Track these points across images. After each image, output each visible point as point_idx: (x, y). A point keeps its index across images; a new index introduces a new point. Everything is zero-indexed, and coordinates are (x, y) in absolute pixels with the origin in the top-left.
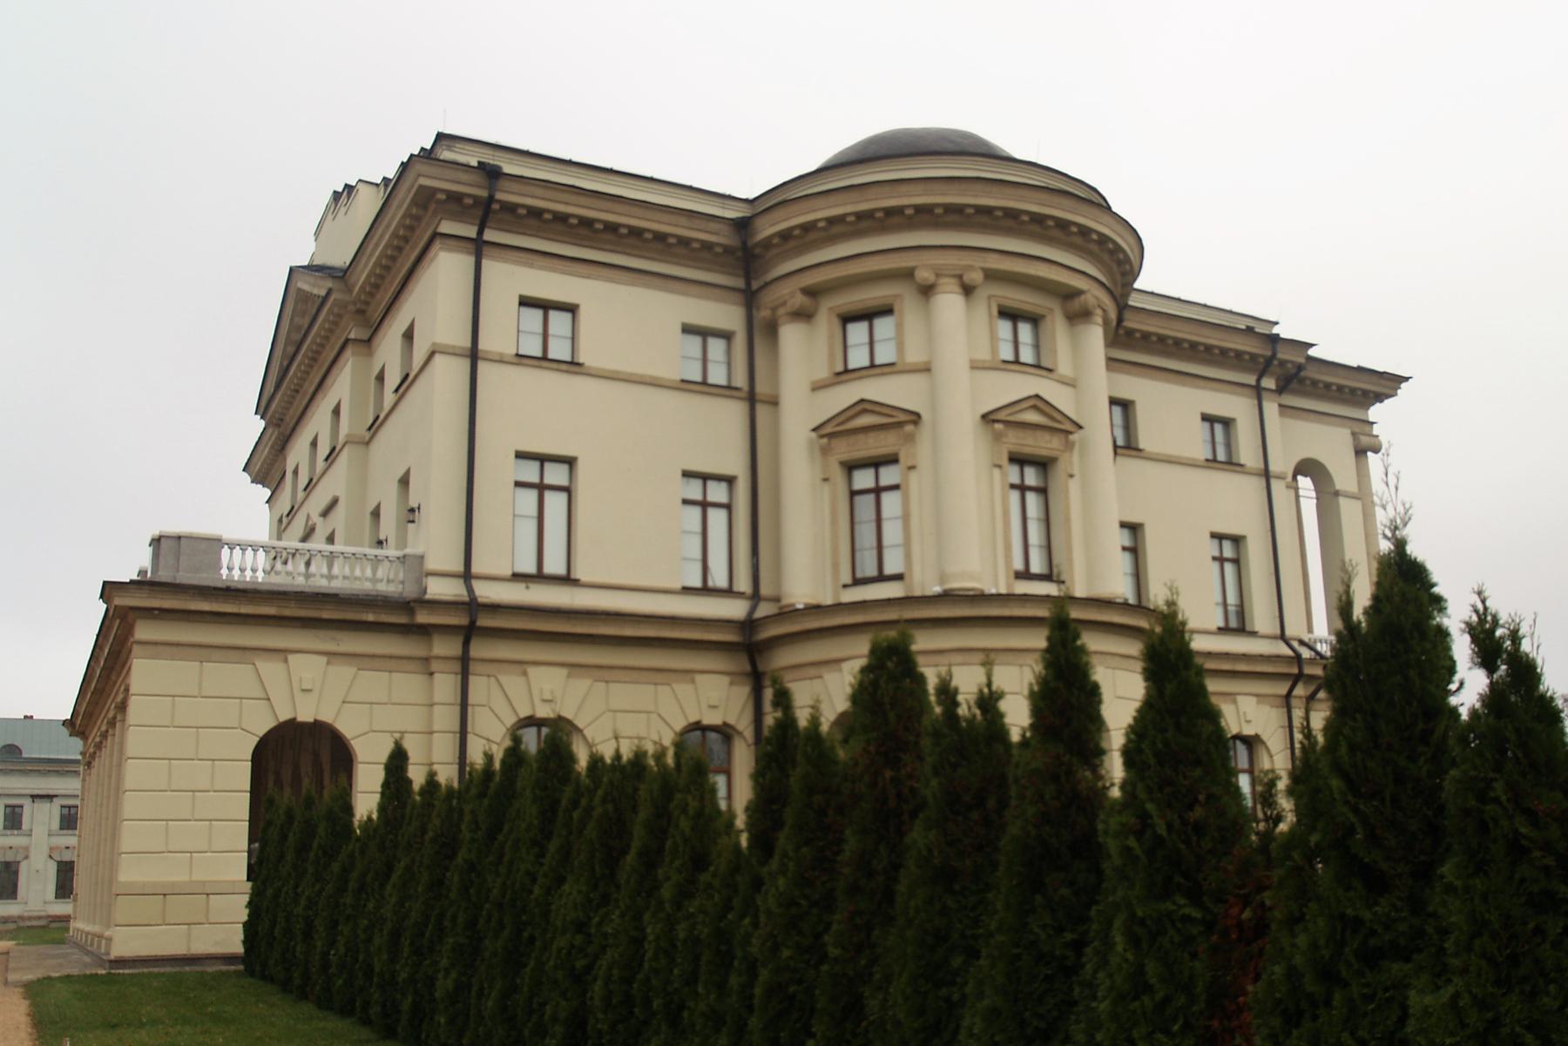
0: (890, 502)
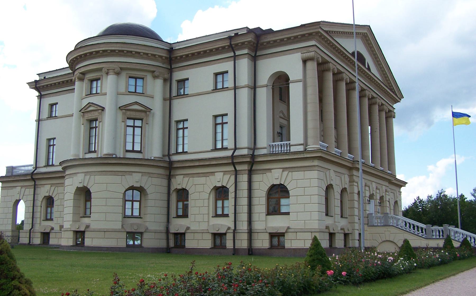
0: (138, 131)
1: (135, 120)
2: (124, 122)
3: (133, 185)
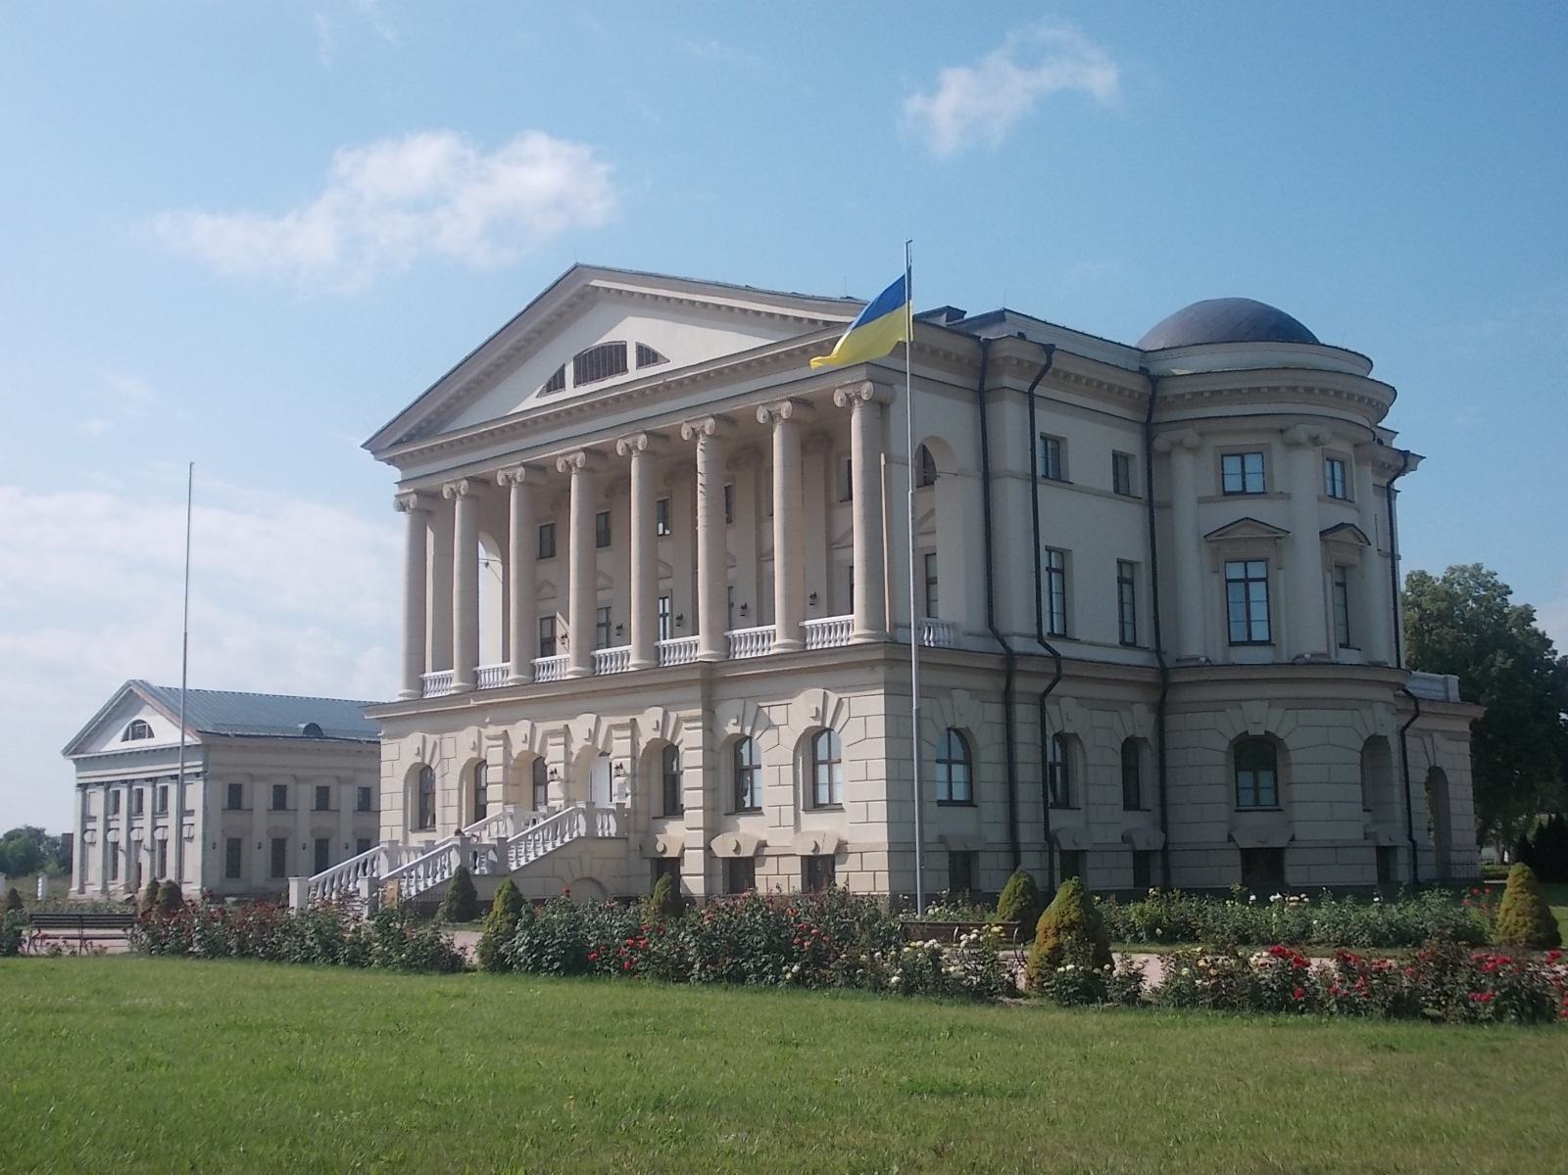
0: (1257, 591)
1: (1249, 564)
2: (1218, 572)
3: (1247, 732)
